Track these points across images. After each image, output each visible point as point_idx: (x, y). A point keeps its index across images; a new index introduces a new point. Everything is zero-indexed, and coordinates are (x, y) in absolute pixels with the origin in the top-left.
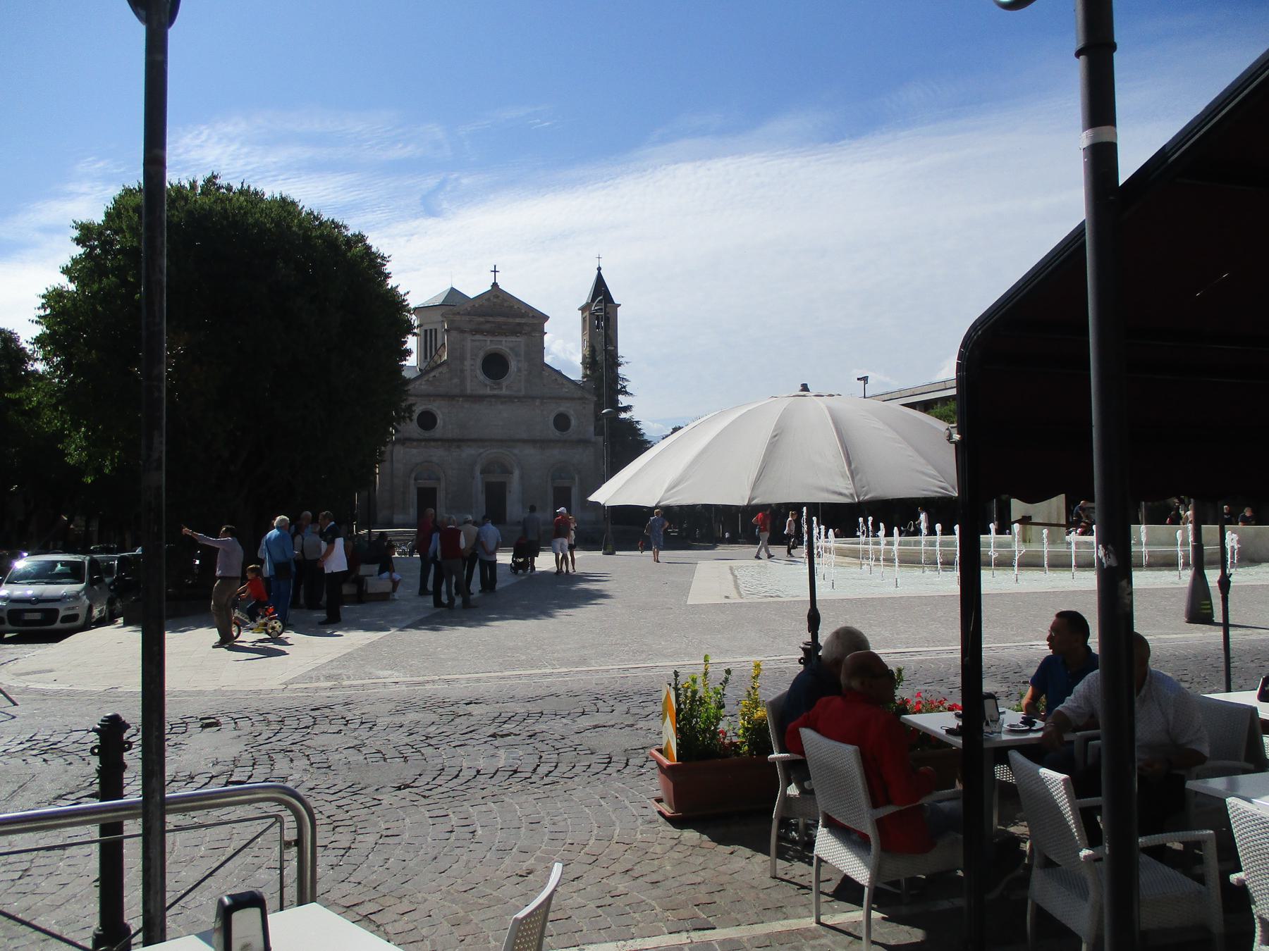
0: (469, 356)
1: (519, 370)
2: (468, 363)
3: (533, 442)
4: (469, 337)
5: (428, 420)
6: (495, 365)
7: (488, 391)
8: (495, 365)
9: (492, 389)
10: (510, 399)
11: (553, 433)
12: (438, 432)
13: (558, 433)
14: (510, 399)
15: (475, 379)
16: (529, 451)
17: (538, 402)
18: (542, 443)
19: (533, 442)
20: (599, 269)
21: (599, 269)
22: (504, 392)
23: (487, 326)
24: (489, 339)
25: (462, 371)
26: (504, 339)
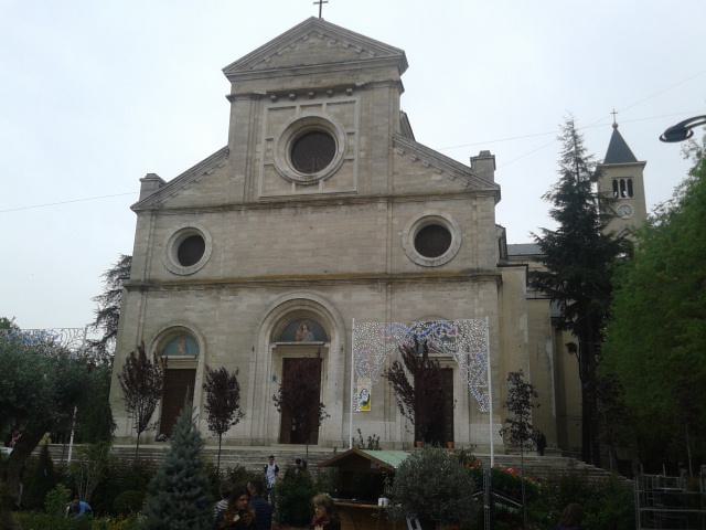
0: (263, 136)
1: (349, 150)
2: (260, 148)
3: (370, 280)
4: (267, 105)
5: (190, 247)
6: (312, 145)
7: (293, 191)
8: (312, 145)
9: (299, 184)
10: (331, 202)
11: (410, 259)
12: (205, 268)
13: (421, 259)
14: (331, 202)
15: (276, 171)
16: (363, 295)
17: (381, 206)
18: (392, 281)
19: (370, 280)
20: (615, 126)
21: (615, 126)
22: (322, 189)
23: (297, 84)
24: (298, 103)
25: (250, 161)
26: (324, 101)
